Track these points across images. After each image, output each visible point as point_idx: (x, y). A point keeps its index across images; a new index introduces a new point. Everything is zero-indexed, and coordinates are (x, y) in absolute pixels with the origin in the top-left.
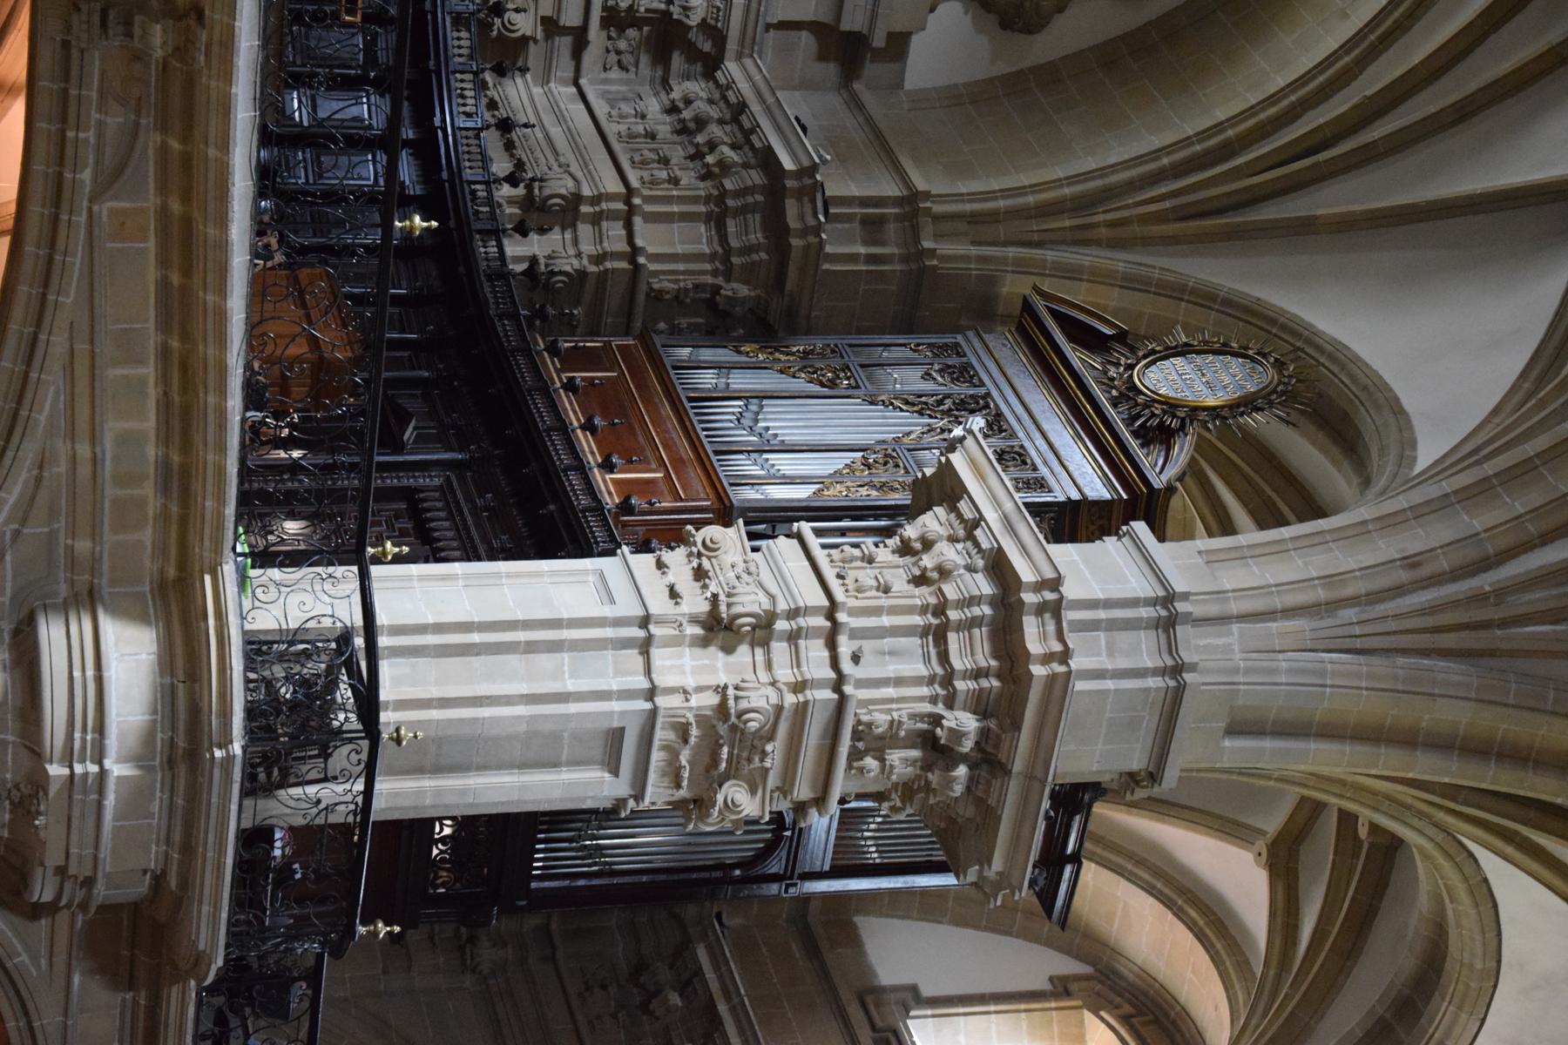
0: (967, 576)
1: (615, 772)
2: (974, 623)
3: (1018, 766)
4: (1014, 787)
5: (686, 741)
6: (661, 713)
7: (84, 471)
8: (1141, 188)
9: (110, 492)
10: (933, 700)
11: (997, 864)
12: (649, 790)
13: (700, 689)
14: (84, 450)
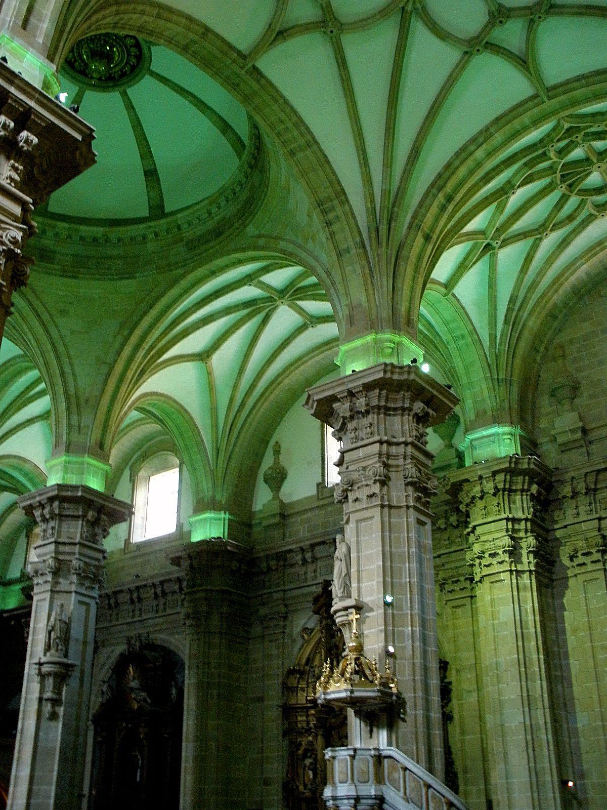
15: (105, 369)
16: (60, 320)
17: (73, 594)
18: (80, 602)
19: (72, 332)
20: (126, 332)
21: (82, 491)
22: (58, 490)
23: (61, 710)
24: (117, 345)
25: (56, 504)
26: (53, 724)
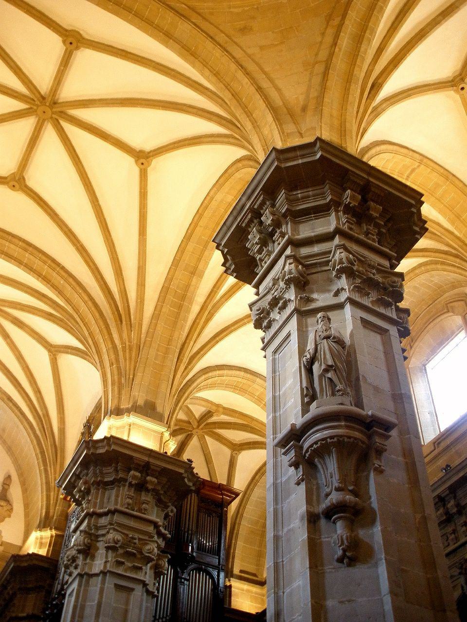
0: (89, 475)
2: (101, 473)
3: (146, 459)
4: (152, 460)
5: (123, 563)
6: (112, 570)
8: (48, 475)
10: (124, 486)
11: (182, 471)
12: (142, 578)
13: (107, 557)
15: (319, 68)
16: (242, 40)
17: (348, 307)
18: (365, 323)
19: (262, 48)
20: (336, 21)
21: (321, 148)
22: (278, 159)
23: (376, 535)
24: (329, 39)
25: (282, 196)
26: (359, 571)
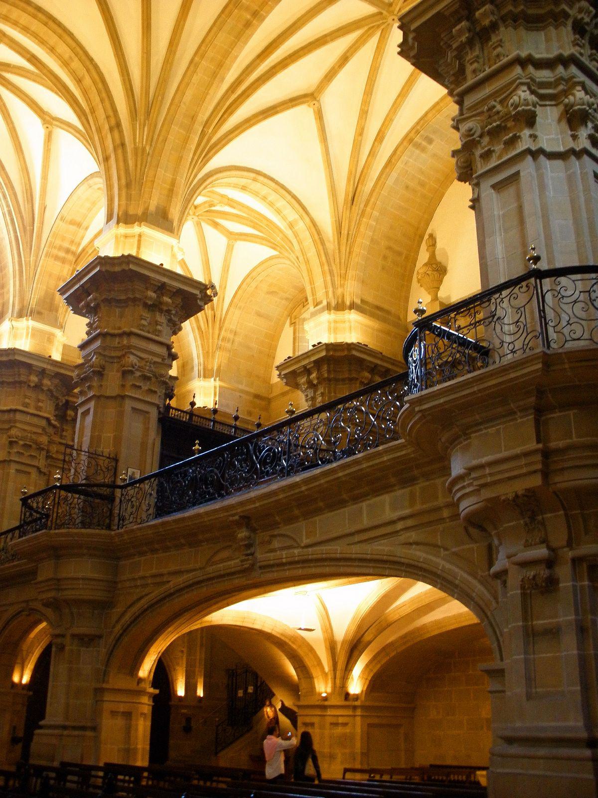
1: (517, 174)
7: (410, 522)
9: (418, 507)
14: (400, 526)
